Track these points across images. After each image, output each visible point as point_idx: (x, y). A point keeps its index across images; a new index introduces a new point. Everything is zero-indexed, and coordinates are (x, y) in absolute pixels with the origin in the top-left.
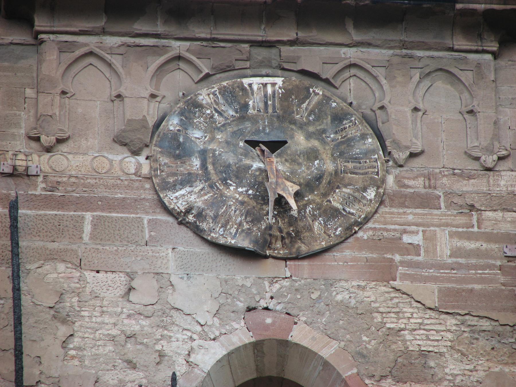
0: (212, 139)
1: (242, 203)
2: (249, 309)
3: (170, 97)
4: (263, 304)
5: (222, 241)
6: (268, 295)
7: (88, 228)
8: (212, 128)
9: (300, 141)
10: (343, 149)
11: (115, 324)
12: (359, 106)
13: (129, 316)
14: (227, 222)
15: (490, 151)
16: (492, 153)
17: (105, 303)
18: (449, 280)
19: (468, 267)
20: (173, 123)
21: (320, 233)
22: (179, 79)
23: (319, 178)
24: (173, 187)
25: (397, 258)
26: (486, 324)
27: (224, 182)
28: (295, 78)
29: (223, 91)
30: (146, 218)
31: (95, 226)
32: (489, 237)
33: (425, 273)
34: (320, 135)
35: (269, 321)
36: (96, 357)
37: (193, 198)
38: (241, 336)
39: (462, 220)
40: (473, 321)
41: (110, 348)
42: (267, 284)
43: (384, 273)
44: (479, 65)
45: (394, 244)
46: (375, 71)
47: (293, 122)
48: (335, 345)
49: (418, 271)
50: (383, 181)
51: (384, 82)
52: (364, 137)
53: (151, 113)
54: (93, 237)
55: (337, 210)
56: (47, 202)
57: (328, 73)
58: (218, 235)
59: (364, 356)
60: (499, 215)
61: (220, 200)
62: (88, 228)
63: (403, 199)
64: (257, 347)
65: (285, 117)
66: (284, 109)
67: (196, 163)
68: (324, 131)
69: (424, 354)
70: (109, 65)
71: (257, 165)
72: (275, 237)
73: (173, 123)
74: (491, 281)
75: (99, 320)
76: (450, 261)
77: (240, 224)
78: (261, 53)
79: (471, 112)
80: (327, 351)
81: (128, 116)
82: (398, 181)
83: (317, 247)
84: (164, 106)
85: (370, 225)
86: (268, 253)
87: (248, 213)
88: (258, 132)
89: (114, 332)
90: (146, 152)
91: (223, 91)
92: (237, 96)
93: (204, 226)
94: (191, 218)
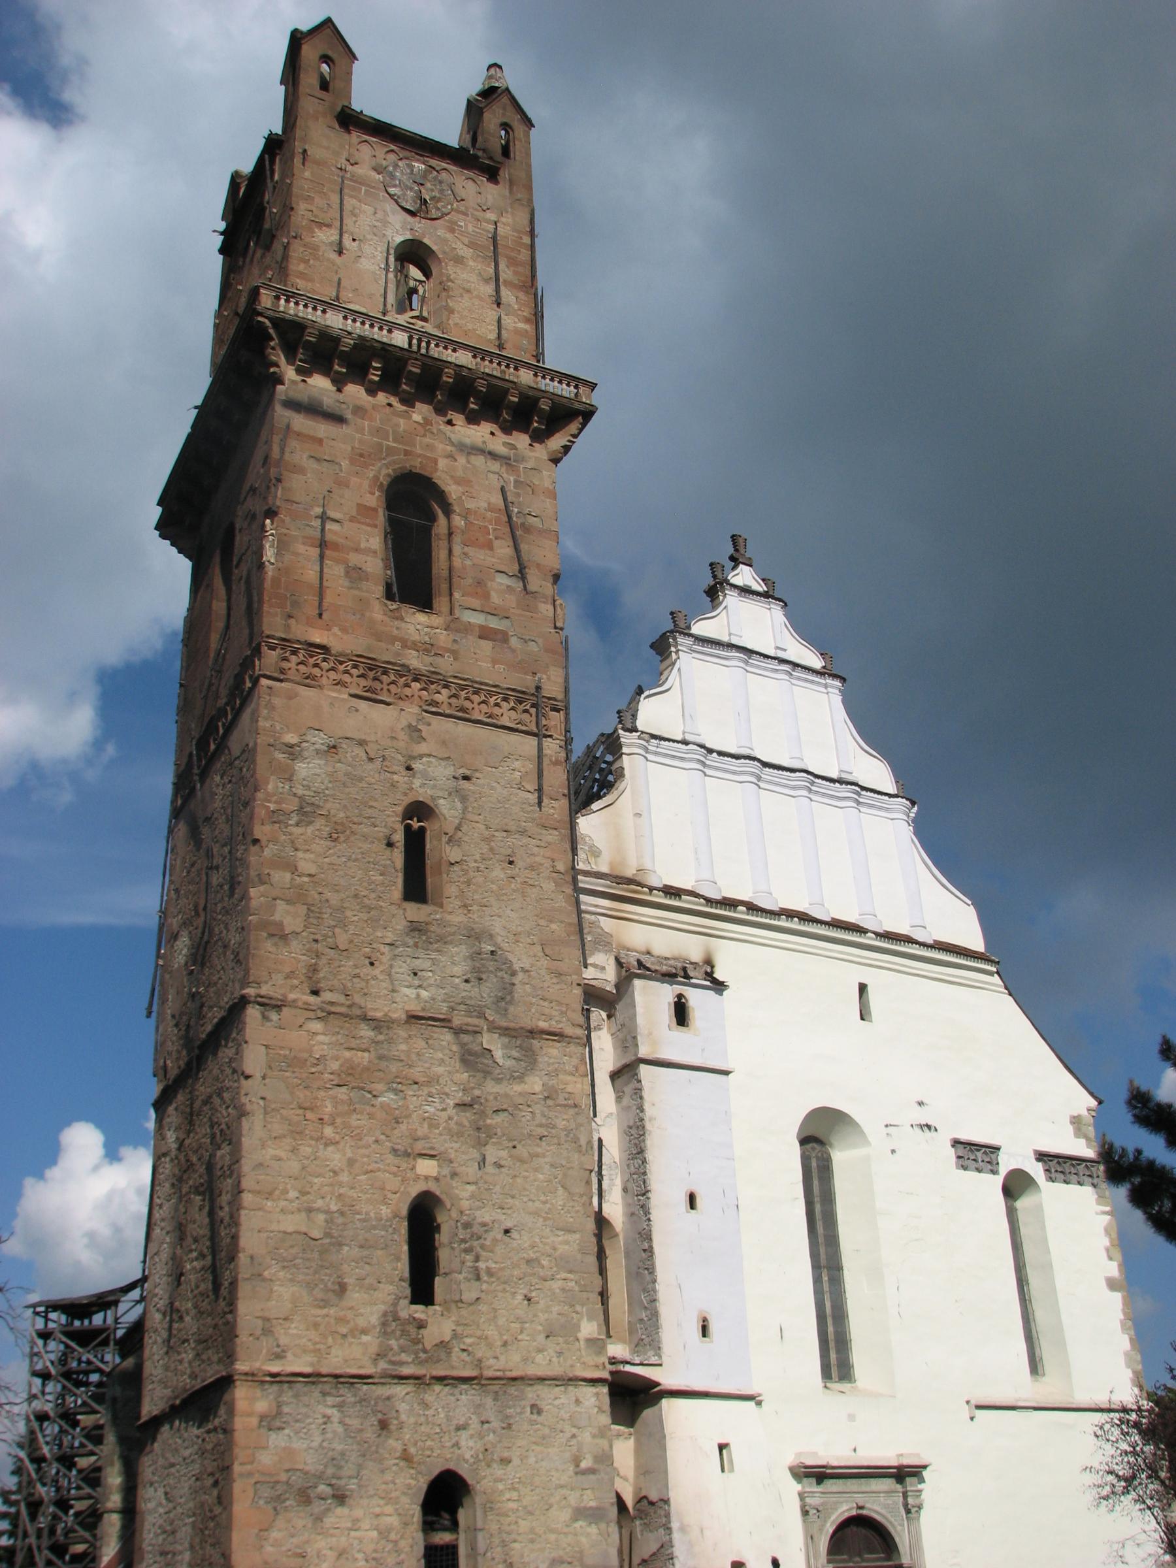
9: (428, 185)
10: (441, 191)
20: (391, 169)
21: (434, 213)
22: (392, 157)
38: (409, 237)
43: (452, 231)
45: (456, 223)
53: (384, 163)
56: (351, 180)
58: (403, 204)
61: (405, 194)
65: (425, 177)
80: (434, 248)
92: (411, 167)
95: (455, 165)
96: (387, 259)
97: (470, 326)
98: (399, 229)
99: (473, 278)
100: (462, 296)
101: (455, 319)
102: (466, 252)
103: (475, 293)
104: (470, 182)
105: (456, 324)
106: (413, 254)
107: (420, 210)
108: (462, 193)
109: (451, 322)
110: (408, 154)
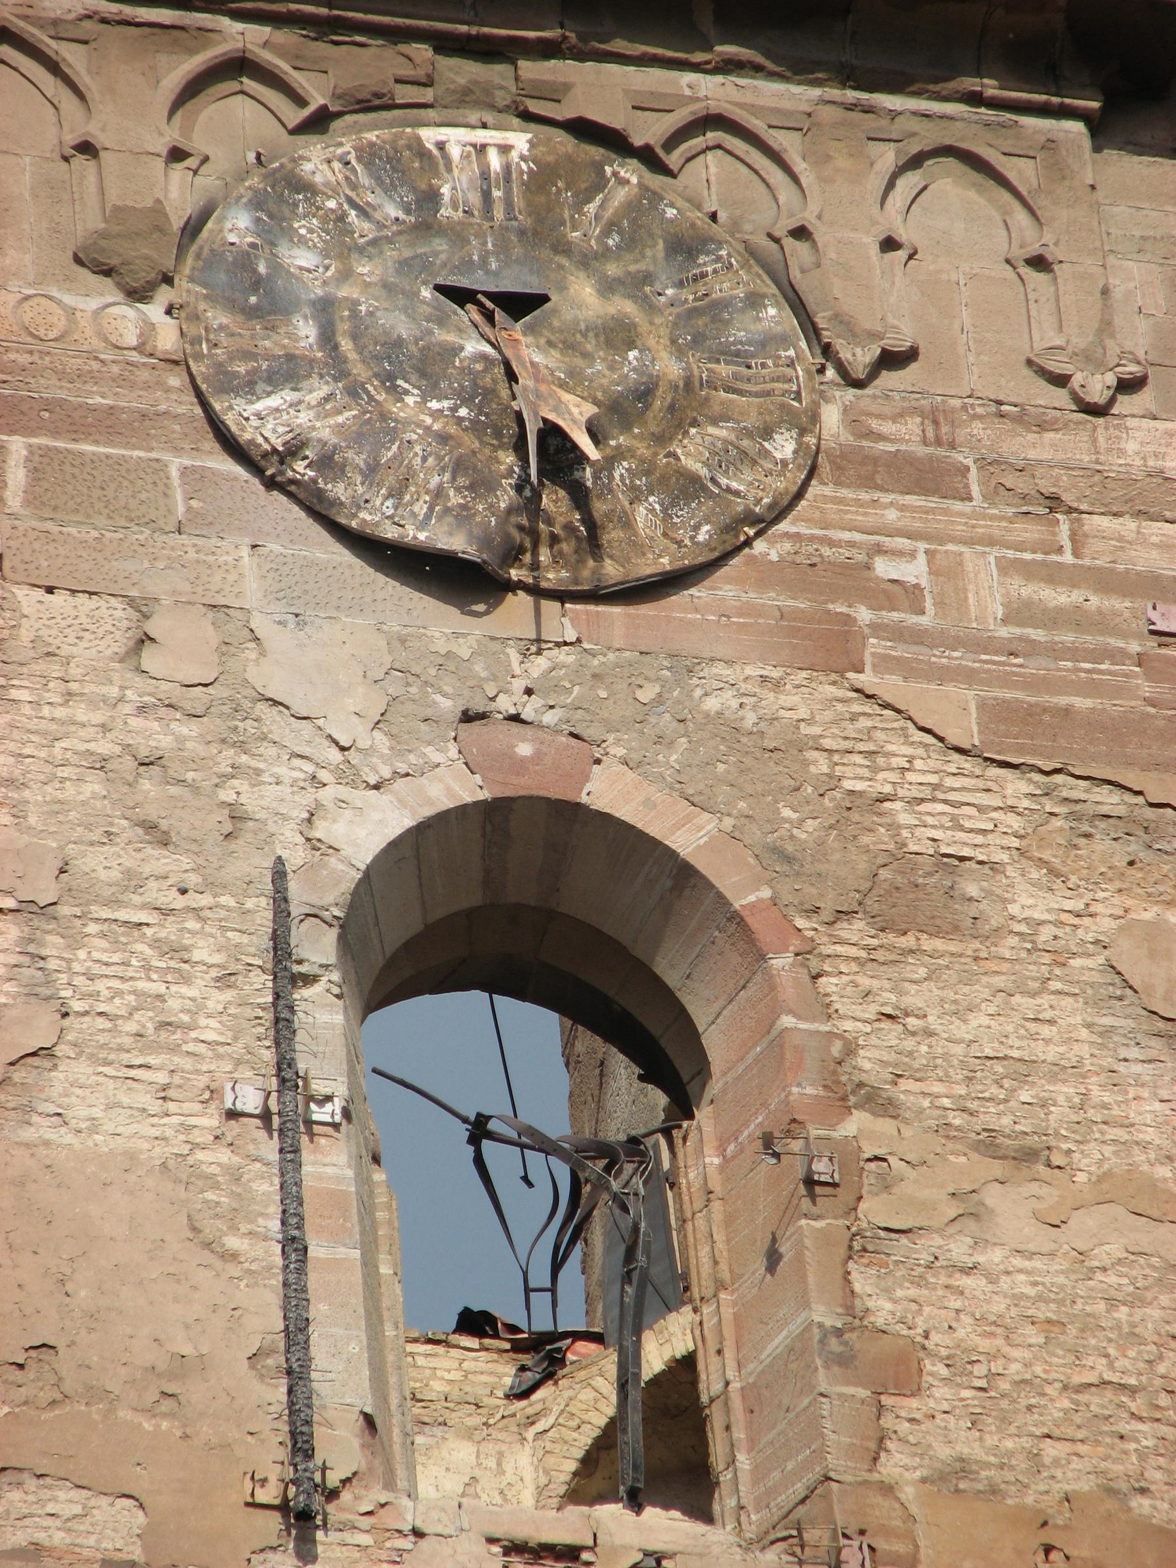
0: (346, 275)
1: (443, 438)
2: (468, 717)
3: (222, 161)
4: (506, 705)
5: (390, 533)
6: (519, 685)
8: (341, 245)
9: (581, 298)
10: (702, 324)
11: (105, 728)
12: (735, 226)
13: (142, 709)
15: (1092, 360)
16: (1100, 366)
17: (74, 671)
18: (1006, 681)
19: (1055, 651)
20: (237, 226)
21: (649, 534)
22: (239, 121)
23: (644, 393)
24: (248, 387)
25: (864, 615)
26: (1109, 800)
27: (388, 380)
28: (560, 137)
29: (368, 155)
30: (175, 464)
31: (35, 473)
32: (1106, 581)
35: (525, 749)
36: (57, 808)
37: (303, 418)
38: (450, 785)
39: (1029, 531)
40: (1079, 790)
41: (94, 786)
42: (514, 655)
43: (831, 650)
44: (1050, 145)
45: (853, 578)
48: (708, 824)
49: (922, 653)
51: (800, 166)
52: (754, 301)
53: (179, 193)
54: (32, 499)
55: (695, 479)
57: (648, 131)
59: (788, 859)
60: (1128, 526)
61: (378, 429)
64: (493, 816)
65: (542, 233)
67: (306, 331)
68: (647, 278)
70: (54, 67)
72: (531, 534)
73: (237, 226)
74: (1118, 691)
75: (60, 713)
76: (1004, 632)
77: (439, 494)
78: (462, 71)
79: (1039, 263)
80: (688, 837)
81: (114, 196)
84: (208, 181)
85: (784, 526)
86: (514, 574)
87: (459, 466)
88: (467, 265)
89: (104, 747)
90: (165, 295)
91: (368, 155)
92: (410, 172)
93: (338, 490)
94: (300, 469)
95: (798, 69)
96: (283, 1026)
97: (1076, 1477)
98: (360, 728)
99: (1066, 1029)
100: (970, 1210)
101: (935, 1428)
103: (1089, 1160)
104: (949, 185)
105: (951, 1478)
106: (530, 919)
108: (877, 301)
109: (896, 1464)
110: (373, 63)
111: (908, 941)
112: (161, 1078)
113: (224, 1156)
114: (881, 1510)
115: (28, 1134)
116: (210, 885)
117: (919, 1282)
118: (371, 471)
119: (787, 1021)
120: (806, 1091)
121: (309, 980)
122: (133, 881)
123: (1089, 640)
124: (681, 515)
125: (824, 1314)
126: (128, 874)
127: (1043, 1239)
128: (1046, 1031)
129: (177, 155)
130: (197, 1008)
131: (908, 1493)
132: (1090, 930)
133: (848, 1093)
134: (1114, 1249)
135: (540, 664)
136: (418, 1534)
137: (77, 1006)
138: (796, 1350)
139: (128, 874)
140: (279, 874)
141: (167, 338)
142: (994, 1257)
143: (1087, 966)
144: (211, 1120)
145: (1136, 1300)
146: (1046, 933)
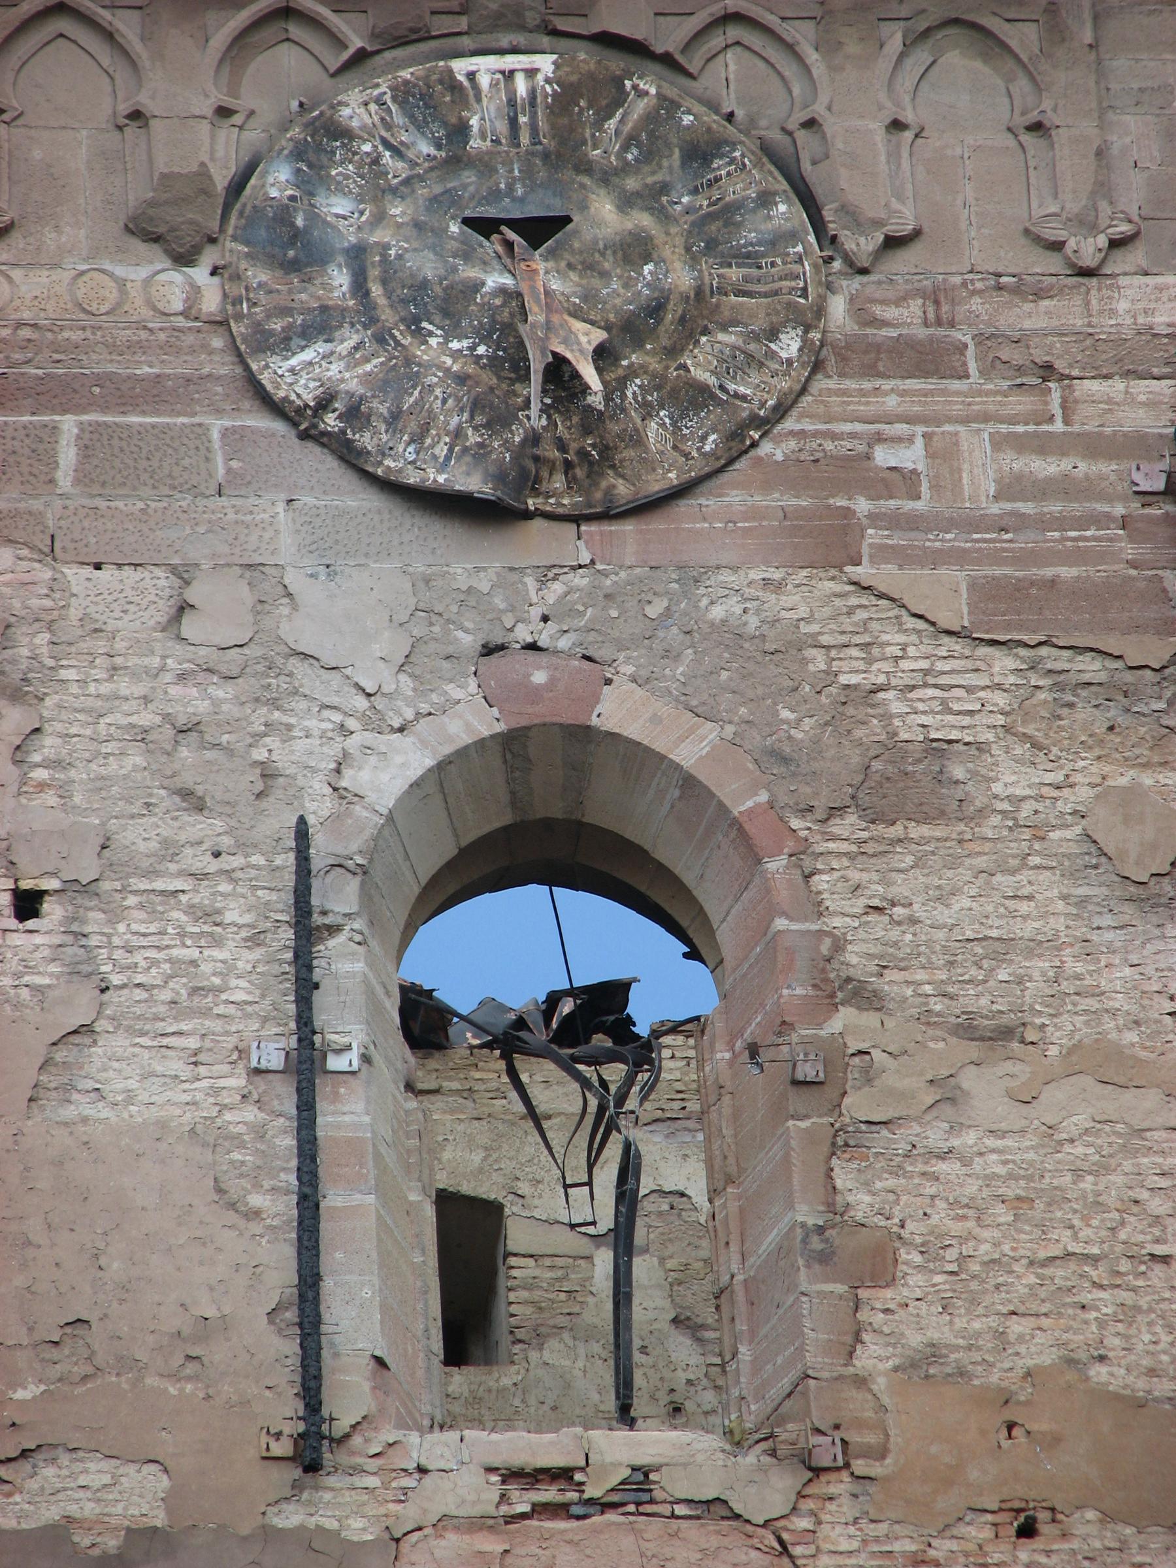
0: (380, 218)
1: (462, 379)
2: (489, 650)
4: (523, 634)
5: (412, 478)
6: (536, 613)
7: (67, 456)
8: (377, 189)
9: (603, 216)
10: (713, 234)
11: (146, 700)
12: (752, 121)
13: (182, 677)
14: (425, 429)
16: (1093, 229)
17: (120, 645)
18: (996, 558)
19: (1043, 523)
23: (656, 309)
24: (284, 344)
25: (862, 506)
26: (1091, 667)
27: (414, 325)
28: (585, 56)
29: (402, 93)
30: (216, 426)
31: (85, 450)
32: (1094, 446)
33: (933, 542)
34: (653, 198)
35: (539, 677)
36: (100, 784)
37: (334, 370)
38: (470, 720)
39: (1021, 403)
41: (136, 759)
42: (531, 583)
43: (829, 545)
45: (854, 471)
46: (789, 31)
47: (585, 167)
48: (710, 733)
49: (918, 539)
50: (820, 311)
51: (812, 56)
52: (766, 199)
54: (82, 477)
55: (704, 389)
57: (669, 37)
58: (403, 461)
59: (785, 760)
61: (403, 374)
62: (67, 456)
63: (874, 357)
64: (512, 744)
65: (564, 155)
66: (560, 135)
67: (340, 279)
68: (664, 188)
69: (938, 749)
70: (109, 36)
71: (495, 280)
72: (549, 462)
73: (277, 181)
74: (1102, 557)
75: (105, 688)
76: (995, 509)
77: (458, 434)
79: (1037, 127)
80: (691, 748)
81: (162, 165)
82: (859, 310)
83: (655, 485)
84: (254, 136)
85: (789, 424)
86: (531, 503)
87: (476, 406)
88: (495, 195)
89: (146, 718)
90: (210, 257)
91: (402, 93)
92: (438, 106)
93: (365, 440)
94: (331, 421)
97: (1039, 1352)
99: (1043, 902)
100: (948, 1095)
101: (912, 1315)
102: (952, 696)
105: (922, 1366)
107: (525, 474)
109: (873, 1357)
111: (896, 831)
112: (193, 1043)
113: (251, 1114)
114: (857, 1404)
115: (69, 1112)
116: (243, 846)
117: (897, 1171)
118: (394, 419)
119: (781, 923)
120: (796, 992)
121: (334, 930)
122: (170, 850)
123: (1076, 508)
124: (690, 426)
125: (807, 1214)
126: (166, 843)
127: (1013, 1116)
128: (1024, 907)
129: (224, 112)
130: (228, 969)
131: (880, 1384)
132: (1069, 800)
133: (839, 990)
134: (1081, 1120)
135: (557, 588)
136: (422, 1470)
137: (116, 979)
138: (782, 1250)
139: (166, 843)
140: (302, 832)
141: (211, 302)
142: (970, 1138)
143: (1064, 837)
144: (238, 1081)
145: (1101, 1169)
146: (1027, 809)
